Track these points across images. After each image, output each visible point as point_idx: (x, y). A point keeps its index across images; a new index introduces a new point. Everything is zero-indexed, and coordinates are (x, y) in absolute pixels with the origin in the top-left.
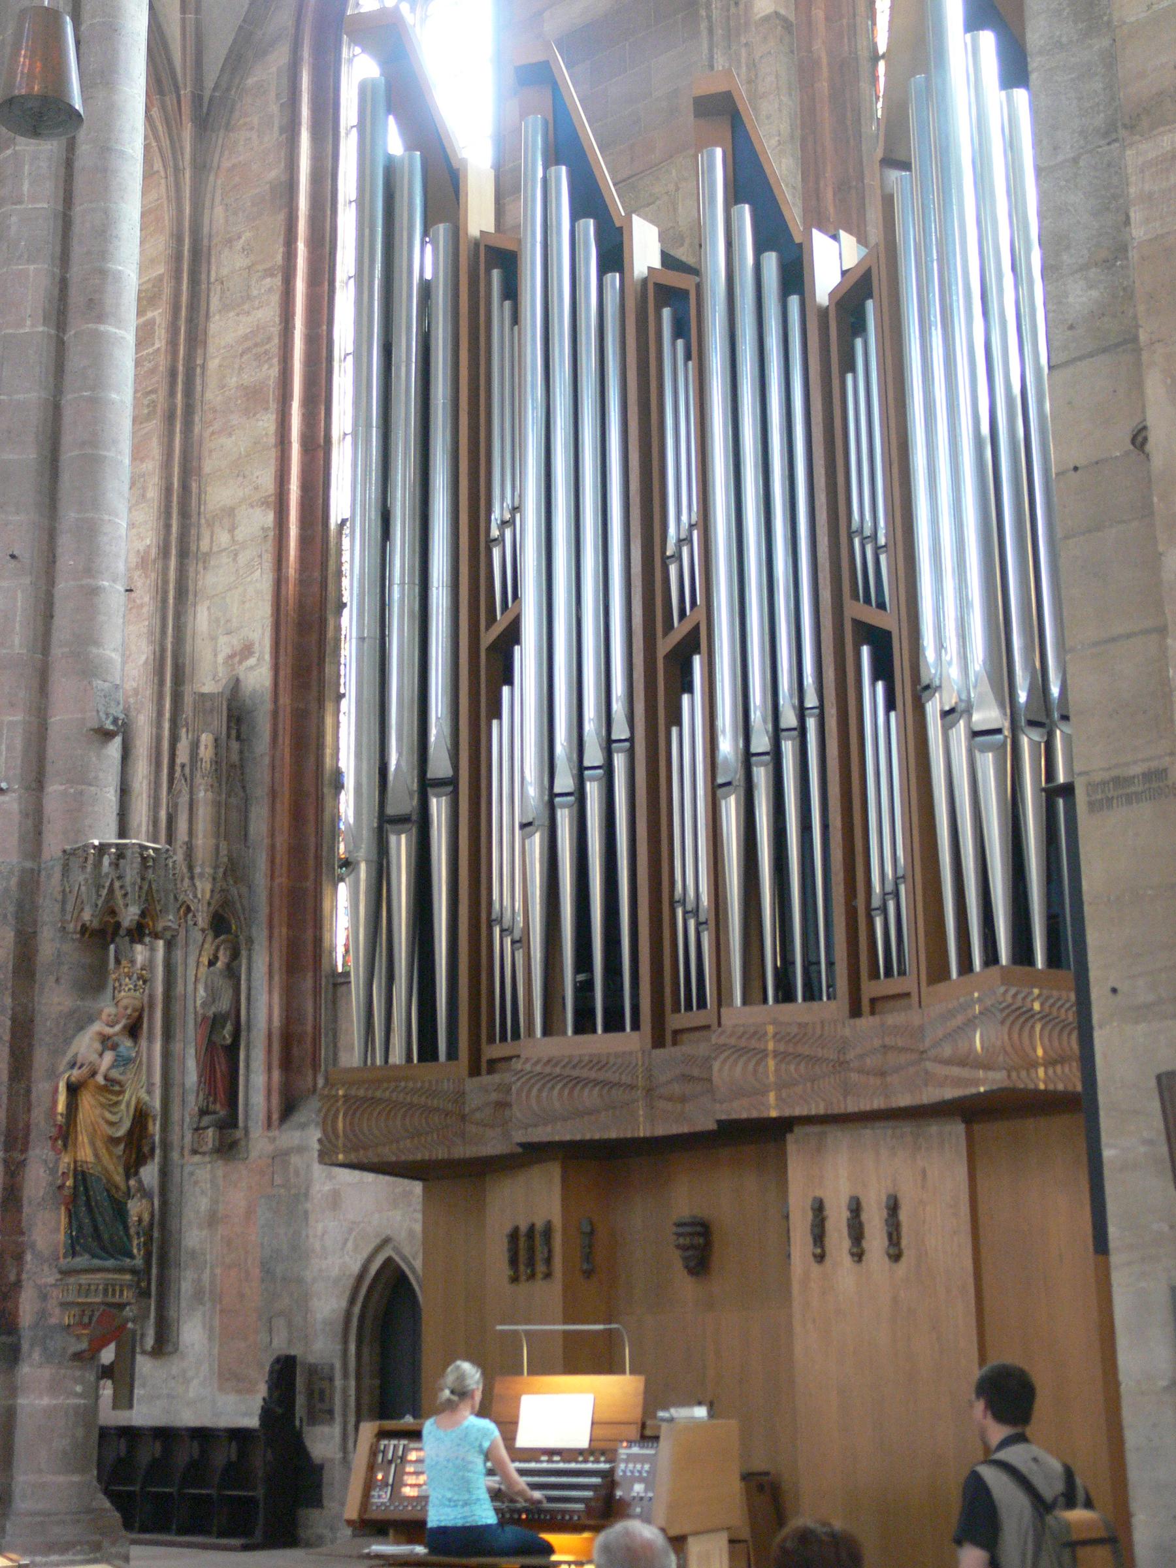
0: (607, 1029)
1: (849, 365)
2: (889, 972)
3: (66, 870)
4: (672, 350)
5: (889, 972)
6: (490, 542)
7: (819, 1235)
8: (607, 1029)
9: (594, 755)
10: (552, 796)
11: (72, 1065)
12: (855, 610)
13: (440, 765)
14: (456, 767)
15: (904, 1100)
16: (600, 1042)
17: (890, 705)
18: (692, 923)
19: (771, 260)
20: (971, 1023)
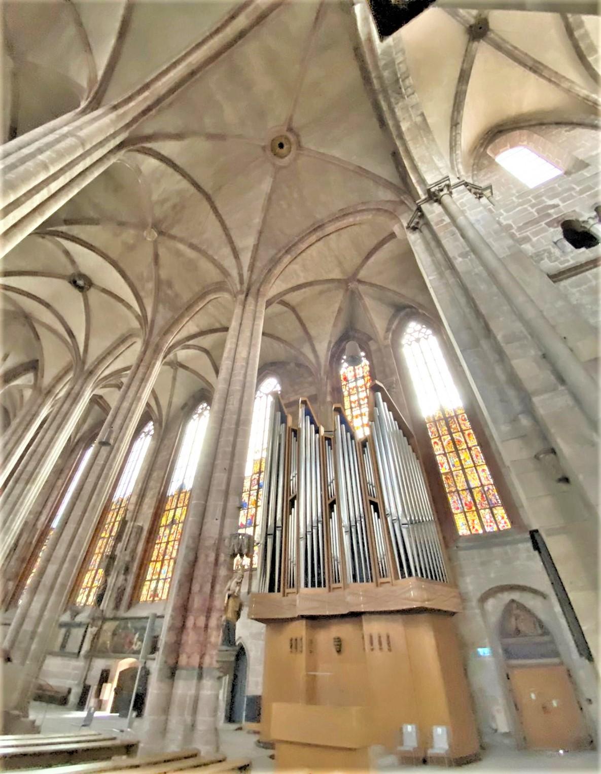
0: (318, 587)
1: (364, 452)
2: (384, 576)
3: (230, 539)
4: (328, 448)
5: (384, 576)
6: (290, 480)
7: (372, 643)
8: (318, 587)
9: (315, 524)
10: (306, 532)
11: (229, 590)
12: (369, 498)
13: (279, 524)
14: (282, 525)
15: (392, 609)
16: (317, 589)
17: (379, 517)
18: (336, 563)
19: (349, 434)
20: (409, 590)
